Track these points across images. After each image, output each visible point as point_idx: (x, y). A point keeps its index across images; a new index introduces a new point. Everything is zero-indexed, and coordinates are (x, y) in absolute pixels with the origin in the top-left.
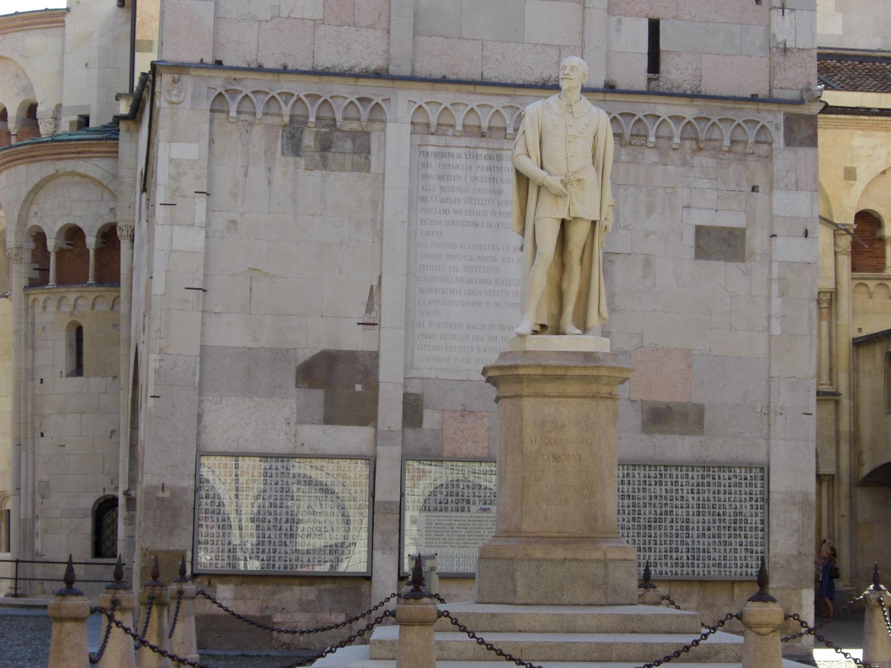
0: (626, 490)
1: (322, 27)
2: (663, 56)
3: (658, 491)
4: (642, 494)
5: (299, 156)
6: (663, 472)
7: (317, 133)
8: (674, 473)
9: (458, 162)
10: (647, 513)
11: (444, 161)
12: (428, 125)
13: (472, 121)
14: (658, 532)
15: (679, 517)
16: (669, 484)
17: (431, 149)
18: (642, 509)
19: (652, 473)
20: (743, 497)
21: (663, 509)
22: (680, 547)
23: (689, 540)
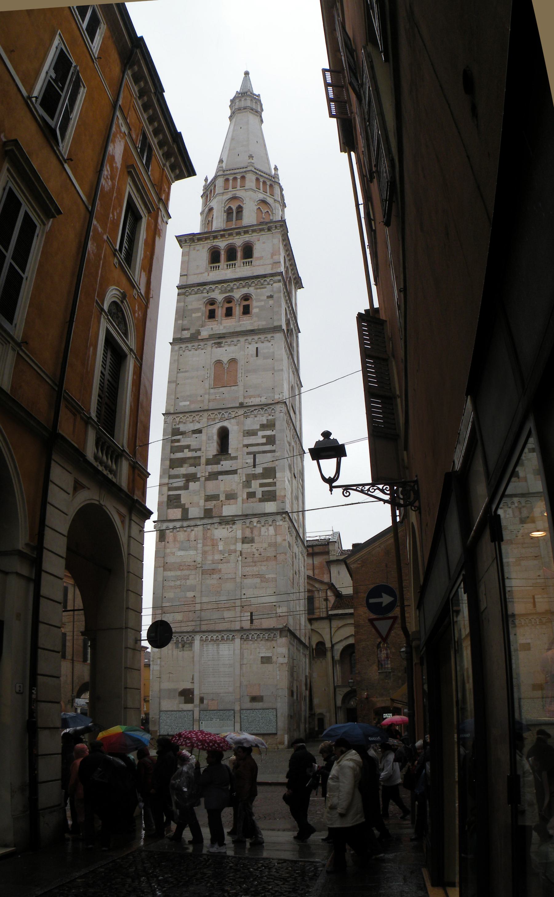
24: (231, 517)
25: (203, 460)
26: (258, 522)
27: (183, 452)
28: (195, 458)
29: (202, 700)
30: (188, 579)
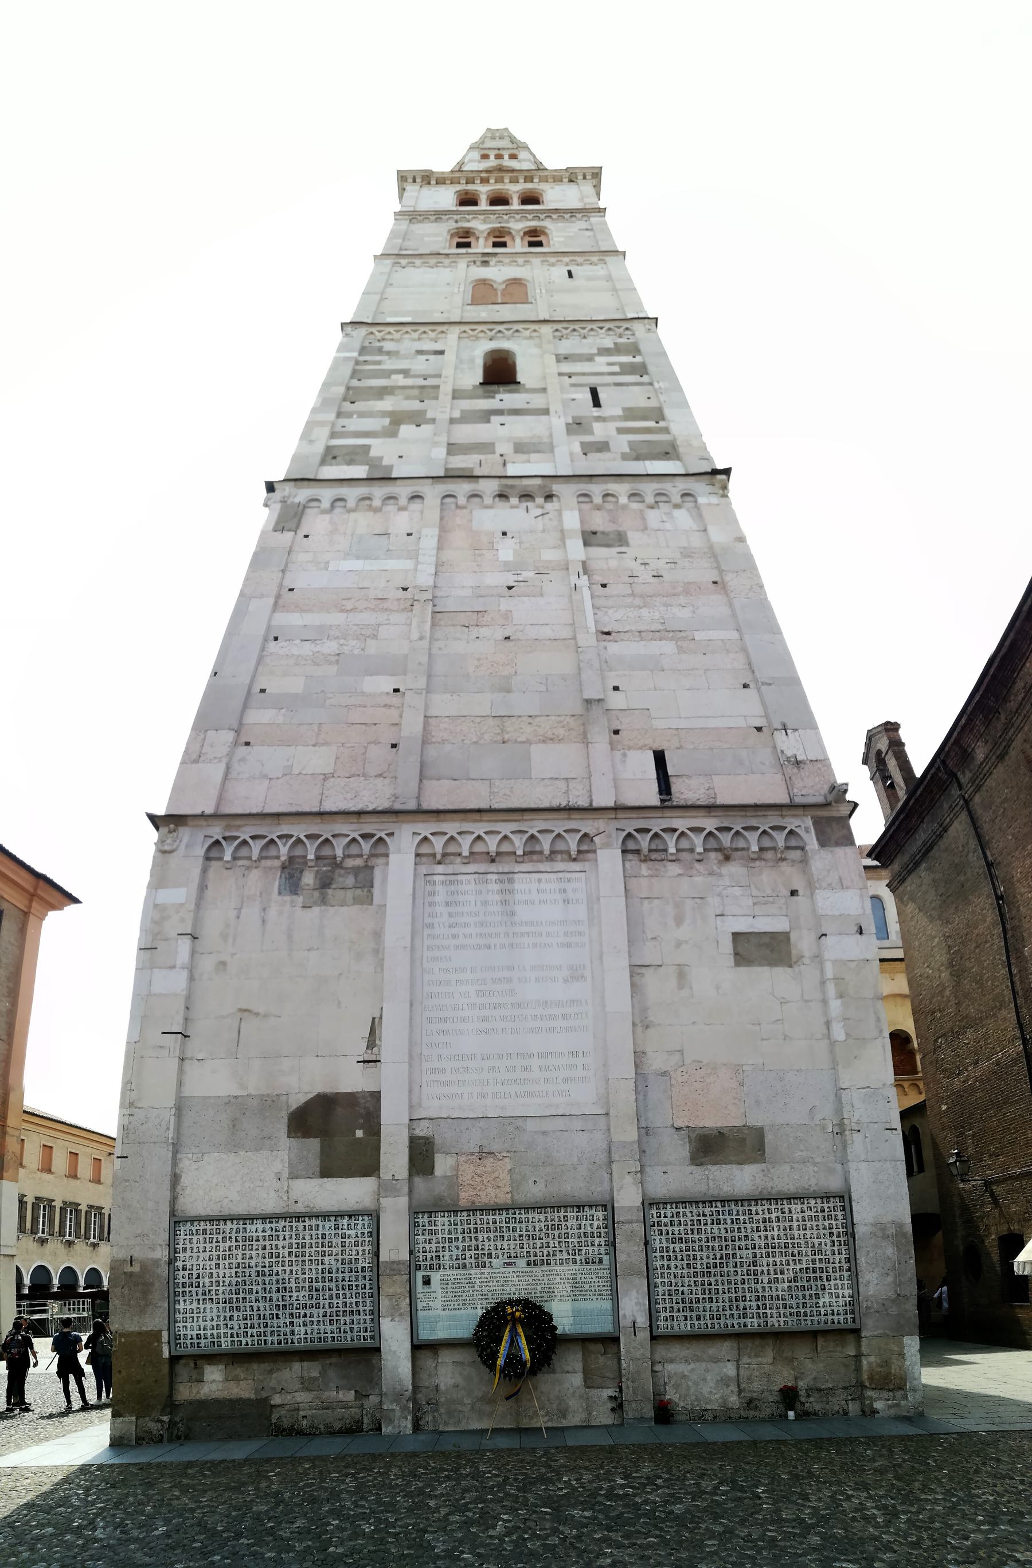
0: (676, 1232)
3: (716, 1231)
4: (696, 1236)
6: (720, 1209)
8: (734, 1209)
10: (704, 1257)
11: (452, 888)
12: (434, 855)
13: (479, 848)
14: (720, 1279)
15: (744, 1260)
16: (729, 1221)
18: (698, 1254)
19: (707, 1211)
20: (822, 1232)
21: (724, 1252)
22: (748, 1295)
23: (759, 1286)
24: (538, 481)
25: (446, 389)
28: (422, 388)
29: (421, 1155)
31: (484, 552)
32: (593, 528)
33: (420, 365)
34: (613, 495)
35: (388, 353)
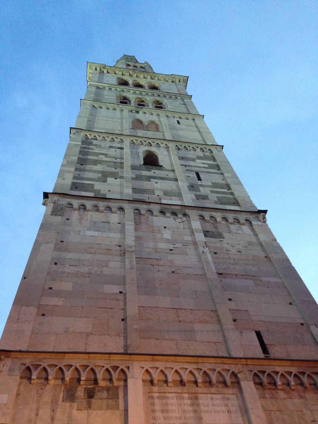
1: (91, 336)
2: (268, 347)
5: (74, 402)
7: (85, 388)
9: (172, 401)
11: (164, 401)
17: (156, 395)
24: (179, 208)
26: (225, 219)
27: (98, 156)
30: (107, 266)
31: (157, 234)
32: (207, 230)
33: (112, 152)
34: (214, 218)
35: (96, 145)
